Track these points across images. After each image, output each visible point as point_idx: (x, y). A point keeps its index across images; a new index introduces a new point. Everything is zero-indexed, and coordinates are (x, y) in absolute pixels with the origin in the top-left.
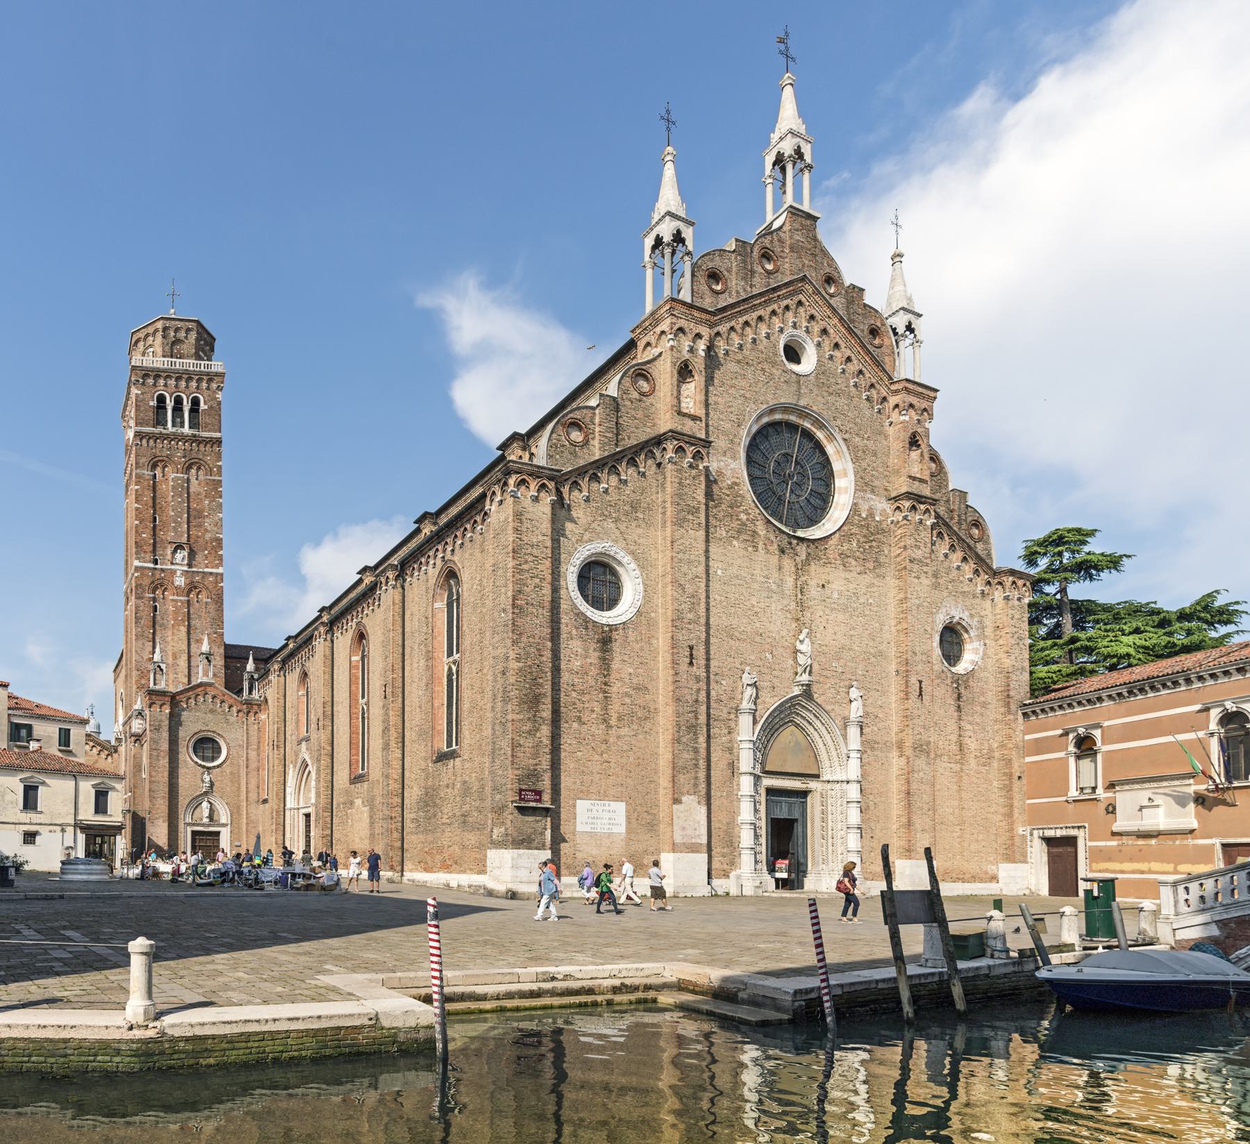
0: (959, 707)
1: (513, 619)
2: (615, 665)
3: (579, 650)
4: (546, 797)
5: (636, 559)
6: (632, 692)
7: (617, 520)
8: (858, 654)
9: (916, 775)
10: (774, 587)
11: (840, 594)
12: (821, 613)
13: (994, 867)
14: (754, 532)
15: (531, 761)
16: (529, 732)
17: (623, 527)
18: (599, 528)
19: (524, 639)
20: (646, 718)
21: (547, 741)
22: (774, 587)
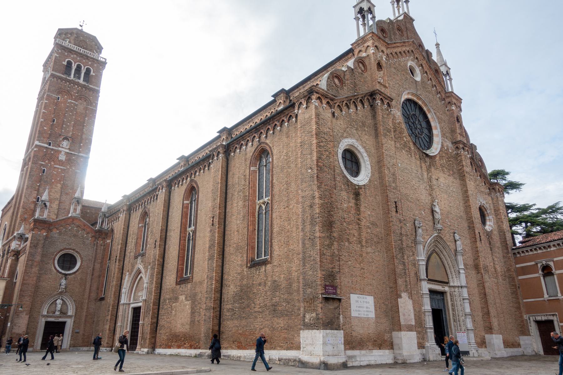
0: (491, 248)
1: (317, 173)
2: (362, 209)
5: (366, 151)
6: (371, 226)
7: (357, 129)
13: (518, 339)
14: (410, 147)
16: (328, 245)
18: (349, 131)
19: (323, 186)
22: (420, 176)
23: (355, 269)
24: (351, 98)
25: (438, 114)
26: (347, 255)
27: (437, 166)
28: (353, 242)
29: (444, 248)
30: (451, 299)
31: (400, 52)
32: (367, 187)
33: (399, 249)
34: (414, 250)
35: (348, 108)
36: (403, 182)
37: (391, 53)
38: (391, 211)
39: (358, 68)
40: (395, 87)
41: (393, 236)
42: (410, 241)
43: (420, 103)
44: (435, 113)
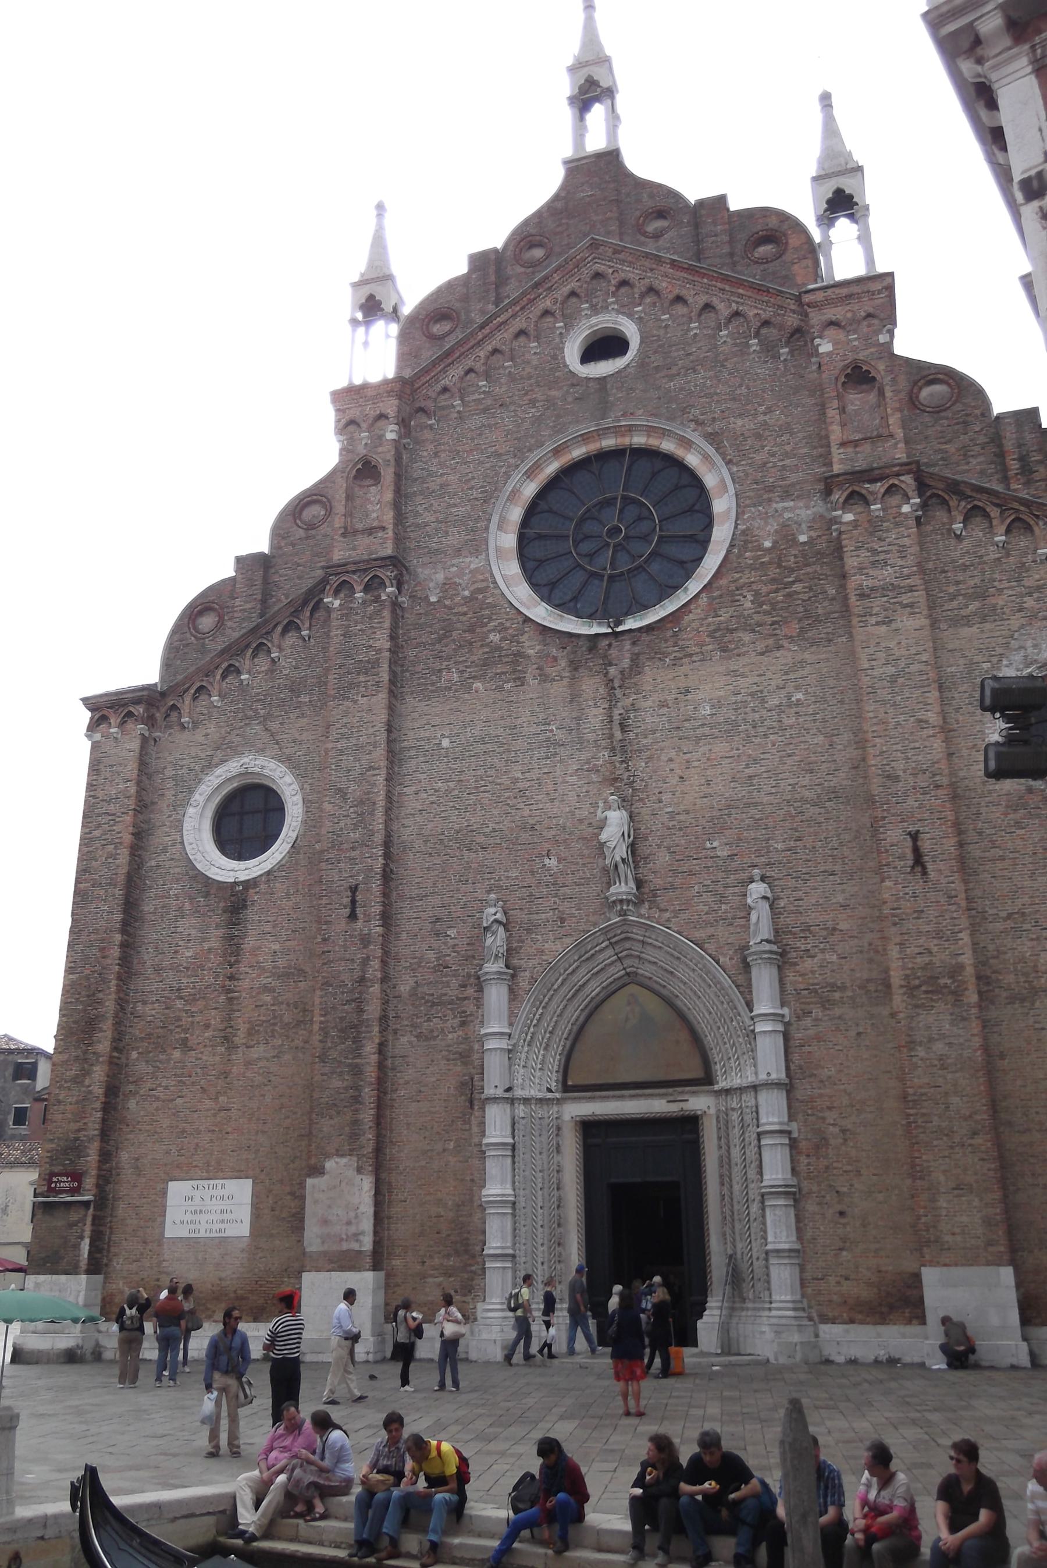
2: (249, 943)
3: (193, 932)
4: (89, 1182)
8: (769, 809)
9: (921, 1052)
10: (560, 735)
11: (717, 704)
12: (673, 754)
14: (519, 654)
15: (74, 1126)
17: (274, 726)
19: (84, 938)
20: (299, 1023)
21: (98, 1091)
23: (196, 1115)
24: (244, 643)
25: (740, 422)
26: (173, 1083)
27: (682, 649)
28: (199, 1044)
29: (672, 955)
30: (719, 1138)
31: (522, 333)
32: (280, 874)
33: (340, 1031)
34: (470, 1008)
35: (239, 672)
36: (456, 792)
37: (470, 370)
38: (327, 923)
39: (295, 528)
40: (468, 481)
41: (321, 997)
42: (454, 983)
43: (639, 440)
44: (713, 438)
